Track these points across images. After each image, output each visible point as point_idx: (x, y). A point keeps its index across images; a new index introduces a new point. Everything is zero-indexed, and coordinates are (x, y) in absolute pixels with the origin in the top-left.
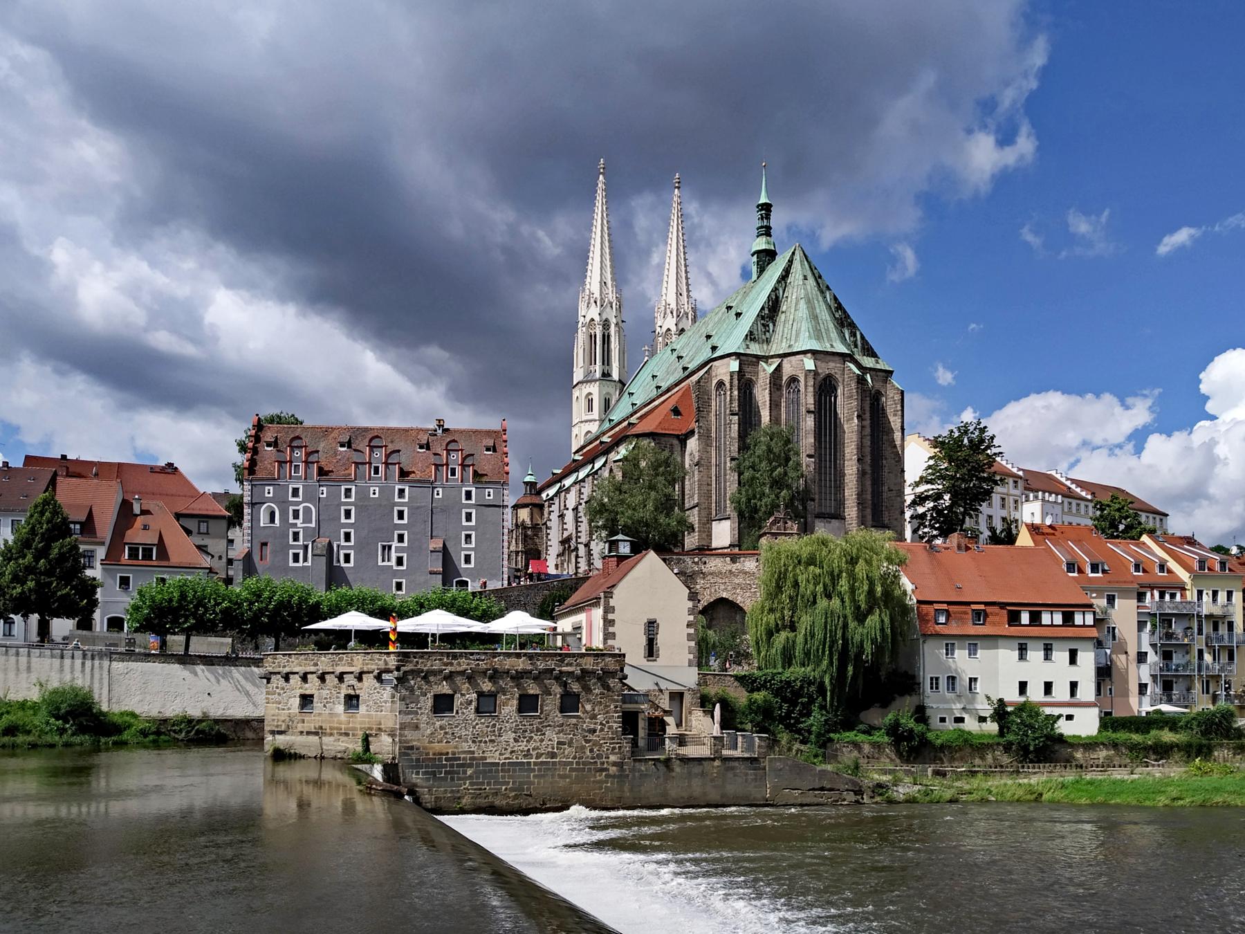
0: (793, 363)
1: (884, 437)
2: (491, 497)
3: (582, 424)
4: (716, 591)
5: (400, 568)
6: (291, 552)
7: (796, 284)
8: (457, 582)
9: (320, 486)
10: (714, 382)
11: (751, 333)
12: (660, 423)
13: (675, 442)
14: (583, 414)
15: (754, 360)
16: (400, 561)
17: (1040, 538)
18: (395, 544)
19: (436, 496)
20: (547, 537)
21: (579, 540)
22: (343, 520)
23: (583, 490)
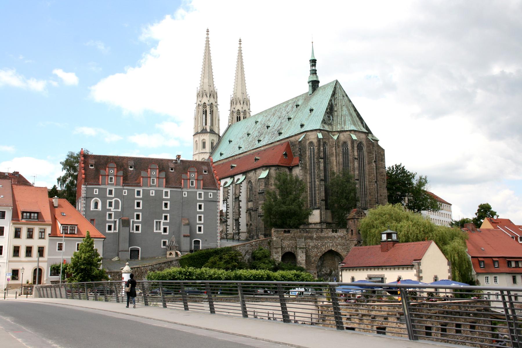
0: (345, 135)
1: (378, 171)
2: (212, 197)
3: (200, 155)
4: (328, 246)
5: (165, 234)
6: (107, 225)
7: (339, 98)
8: (194, 241)
9: (124, 189)
10: (308, 142)
11: (324, 120)
12: (280, 160)
13: (287, 170)
14: (200, 149)
15: (327, 133)
16: (165, 230)
17: (494, 224)
18: (163, 221)
19: (184, 196)
22: (136, 208)
23: (229, 191)
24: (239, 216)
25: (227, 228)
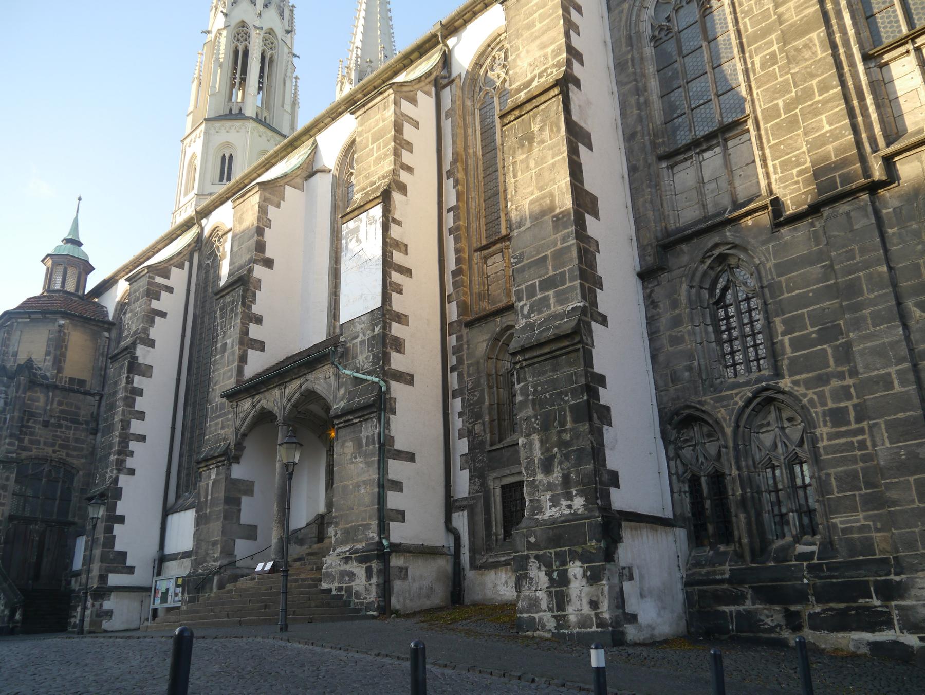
20: (130, 402)
21: (397, 362)
23: (409, 132)
24: (589, 294)
25: (385, 485)
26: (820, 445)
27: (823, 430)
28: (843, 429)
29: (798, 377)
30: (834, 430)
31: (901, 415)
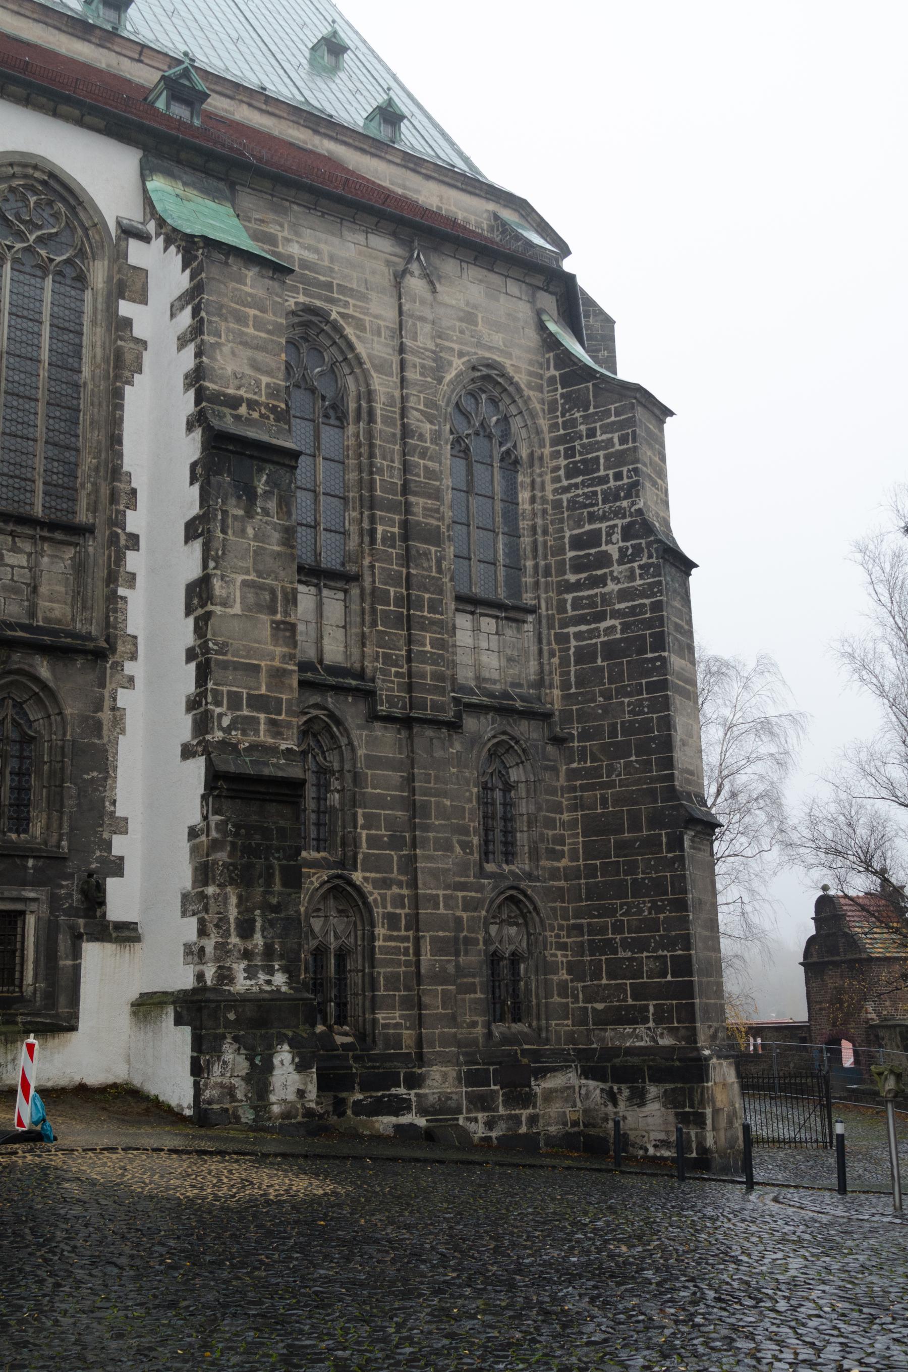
26: (377, 944)
27: (381, 931)
28: (395, 934)
29: (368, 874)
30: (389, 933)
31: (441, 934)
